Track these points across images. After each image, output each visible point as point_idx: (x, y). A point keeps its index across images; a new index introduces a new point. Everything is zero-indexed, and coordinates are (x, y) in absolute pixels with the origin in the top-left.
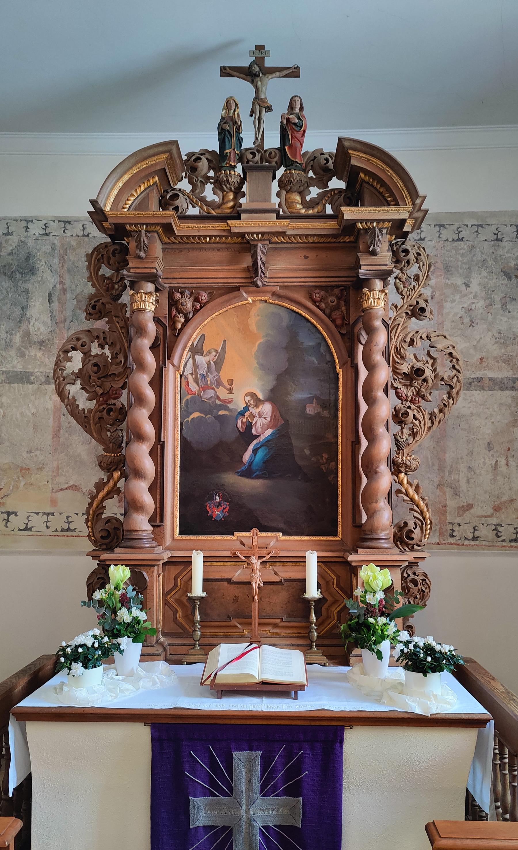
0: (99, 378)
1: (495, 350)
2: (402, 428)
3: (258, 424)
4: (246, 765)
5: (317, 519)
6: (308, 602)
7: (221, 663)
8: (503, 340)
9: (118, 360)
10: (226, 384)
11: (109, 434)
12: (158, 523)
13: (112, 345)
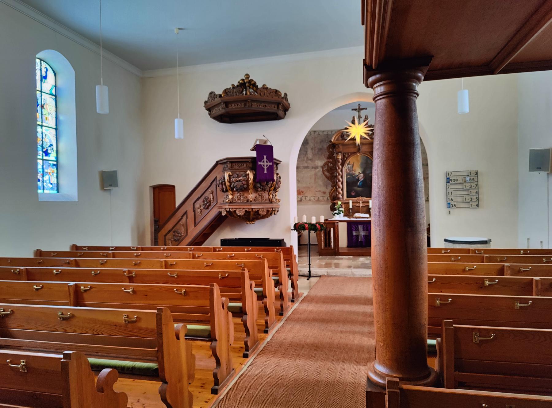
4: (360, 227)
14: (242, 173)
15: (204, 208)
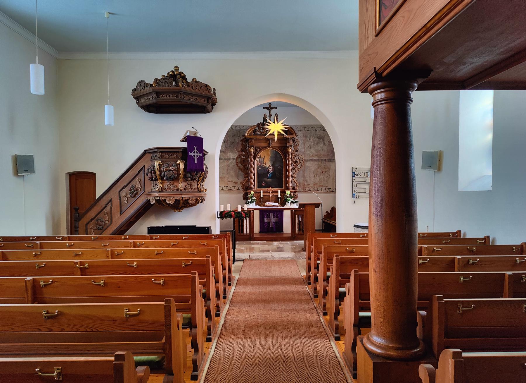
1: (315, 153)
4: (271, 215)
5: (280, 186)
8: (317, 151)
14: (172, 163)
15: (131, 196)
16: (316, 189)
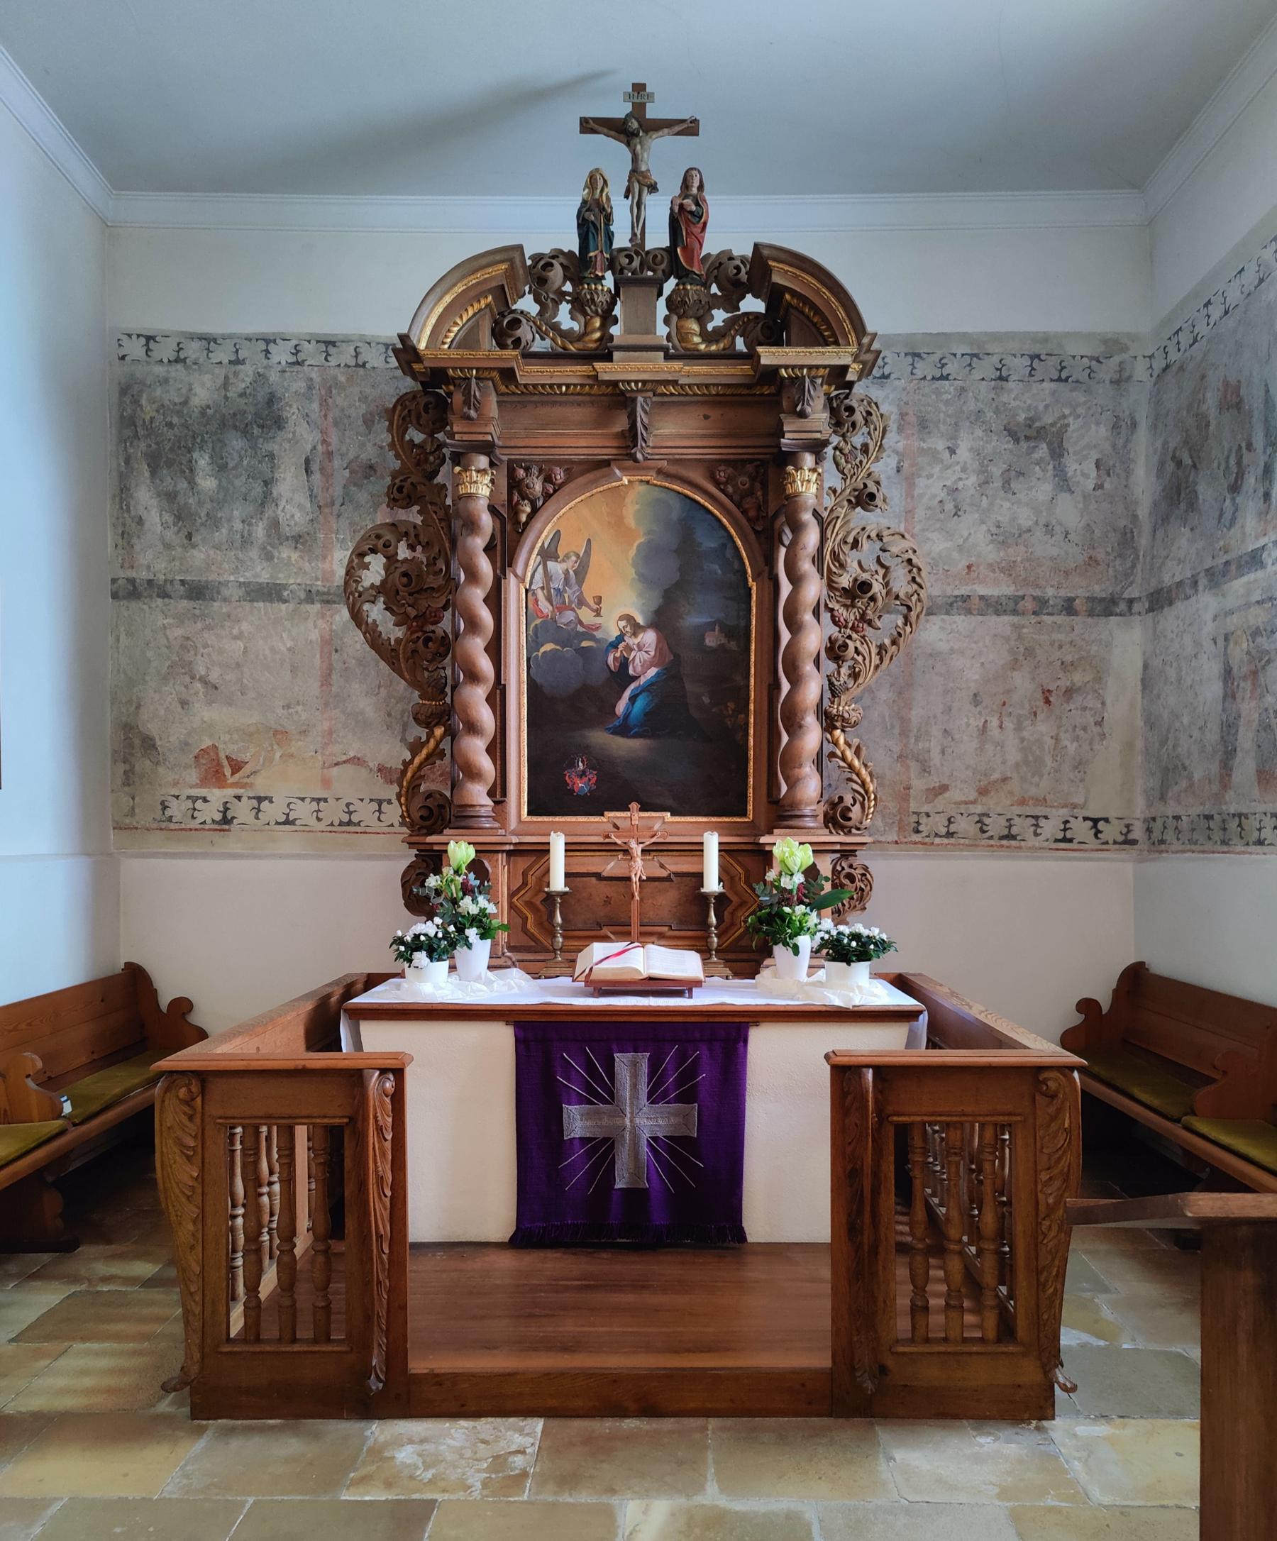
0: (411, 594)
1: (991, 553)
2: (839, 667)
3: (637, 661)
4: (630, 1070)
5: (719, 797)
6: (705, 897)
7: (596, 960)
8: (1002, 538)
9: (437, 568)
10: (591, 602)
11: (426, 674)
12: (498, 798)
13: (427, 546)
16: (996, 826)
